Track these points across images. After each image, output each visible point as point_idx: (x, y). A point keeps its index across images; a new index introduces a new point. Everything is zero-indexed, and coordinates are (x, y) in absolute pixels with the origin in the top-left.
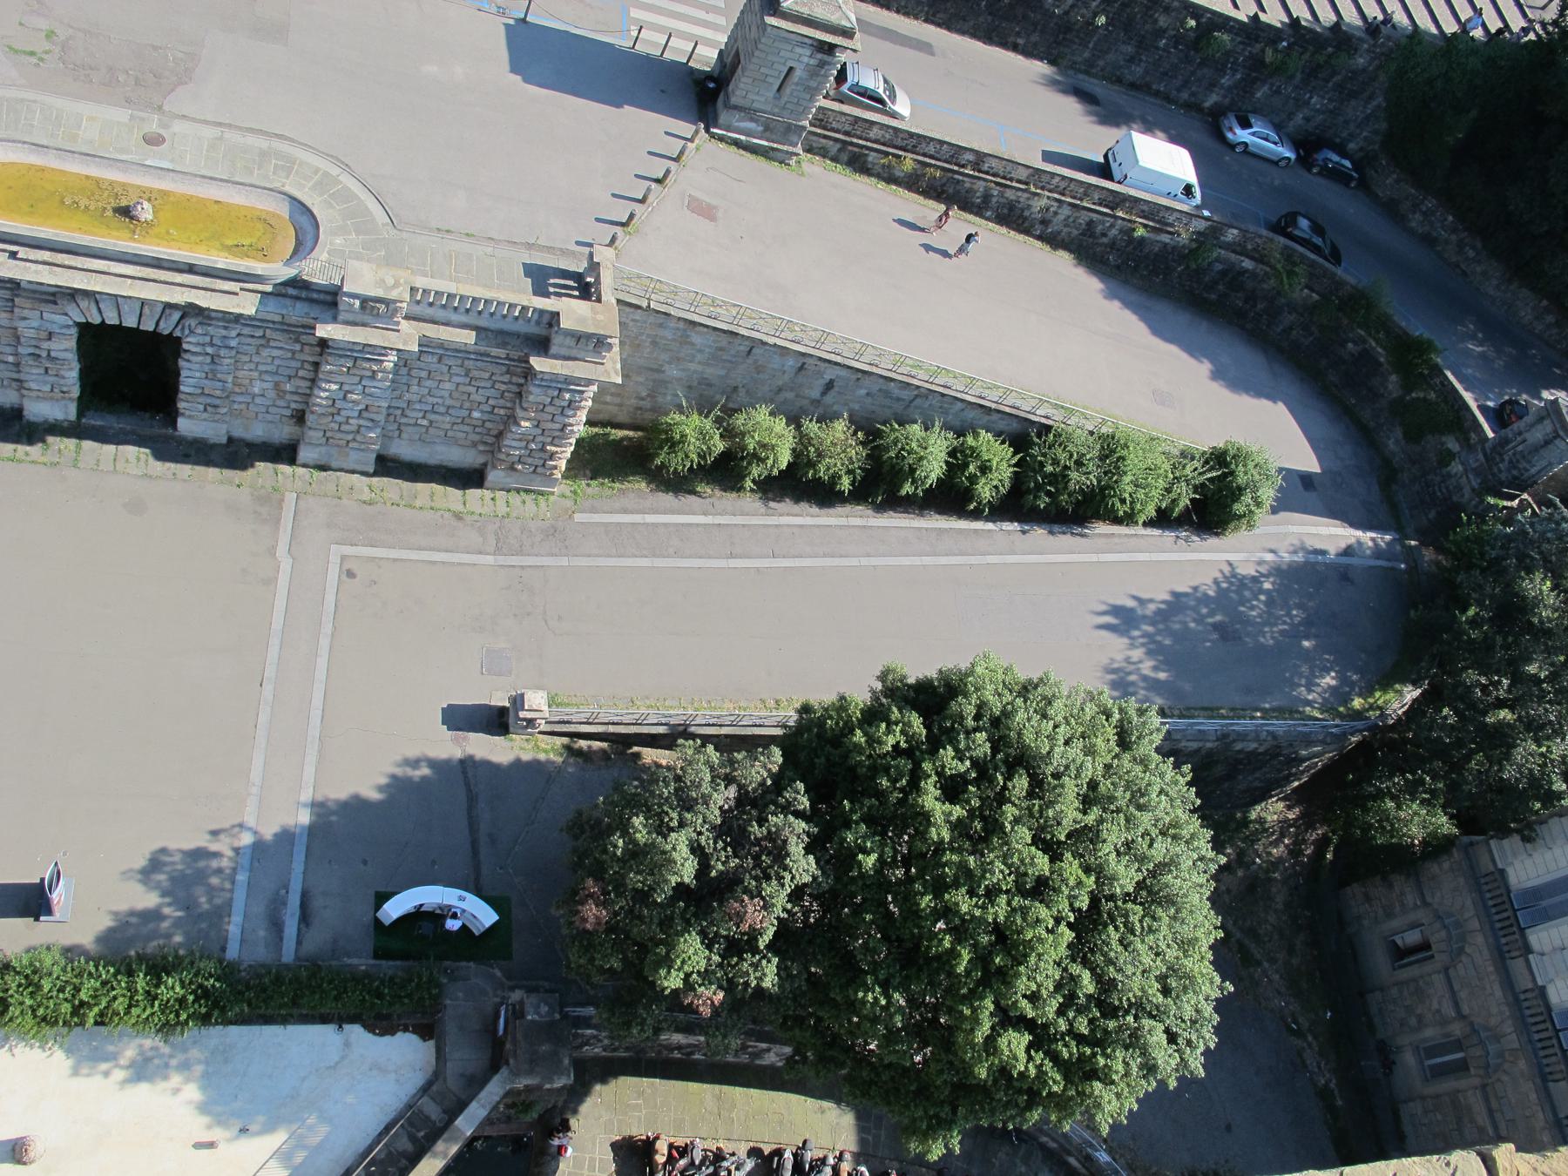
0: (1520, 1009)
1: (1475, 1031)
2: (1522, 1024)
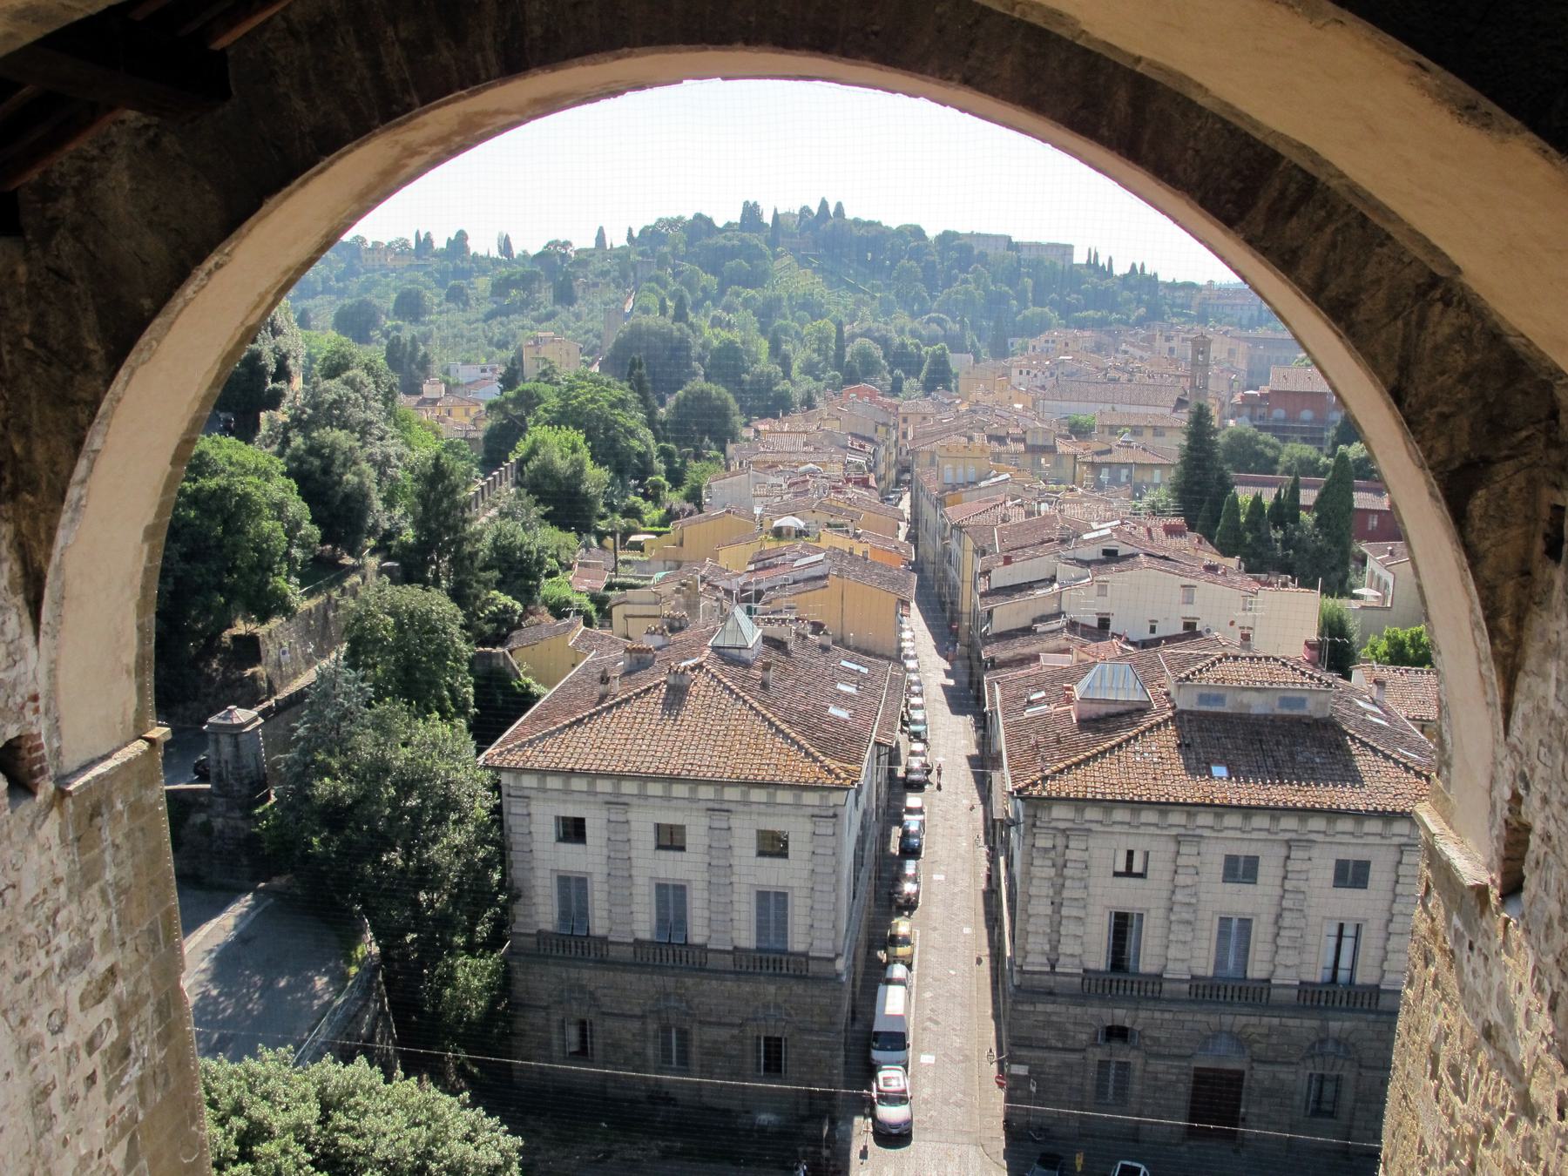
0: (647, 965)
1: (659, 1012)
2: (659, 969)
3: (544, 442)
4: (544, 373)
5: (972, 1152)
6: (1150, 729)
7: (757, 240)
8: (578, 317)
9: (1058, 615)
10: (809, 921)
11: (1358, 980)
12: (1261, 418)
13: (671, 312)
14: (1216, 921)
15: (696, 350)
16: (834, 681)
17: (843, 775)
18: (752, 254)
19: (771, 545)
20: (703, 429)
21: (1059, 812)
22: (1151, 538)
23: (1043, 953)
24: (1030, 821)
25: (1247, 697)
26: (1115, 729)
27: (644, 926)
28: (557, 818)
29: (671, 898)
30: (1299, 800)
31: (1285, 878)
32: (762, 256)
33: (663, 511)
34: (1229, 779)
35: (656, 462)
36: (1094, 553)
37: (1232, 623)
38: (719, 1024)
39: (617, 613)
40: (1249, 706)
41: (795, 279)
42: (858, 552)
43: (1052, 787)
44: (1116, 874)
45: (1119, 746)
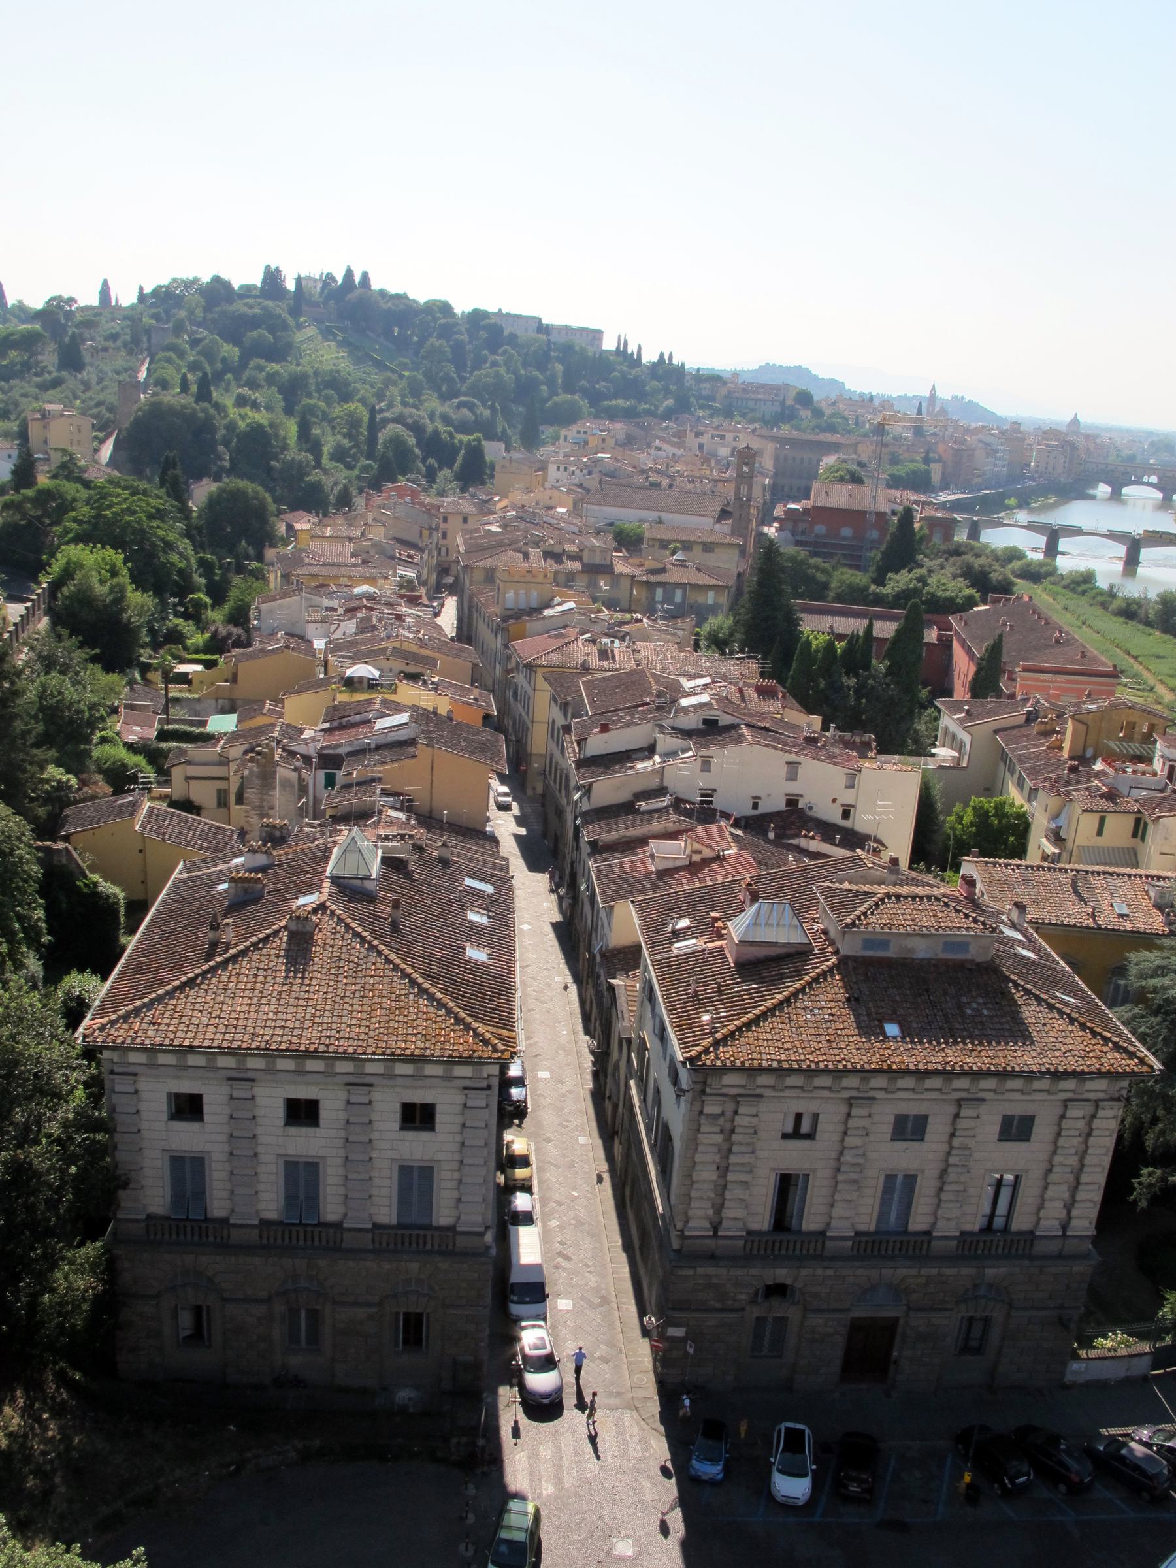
3: (81, 566)
4: (64, 466)
5: (628, 1417)
6: (816, 980)
7: (280, 309)
8: (87, 386)
9: (661, 791)
10: (455, 1194)
11: (1015, 1226)
12: (803, 533)
13: (194, 388)
14: (882, 1179)
15: (221, 433)
16: (463, 908)
17: (501, 1047)
18: (274, 324)
19: (343, 697)
20: (238, 534)
21: (729, 1079)
22: (743, 699)
23: (707, 1218)
24: (699, 1087)
25: (911, 943)
26: (781, 977)
27: (270, 1202)
28: (169, 1095)
29: (302, 1177)
30: (973, 1061)
31: (953, 1135)
32: (285, 327)
33: (207, 635)
34: (903, 1038)
35: (196, 577)
36: (692, 721)
37: (834, 801)
38: (356, 1304)
39: (177, 774)
40: (912, 950)
41: (320, 353)
42: (443, 711)
43: (726, 1053)
44: (785, 1136)
45: (787, 1000)
